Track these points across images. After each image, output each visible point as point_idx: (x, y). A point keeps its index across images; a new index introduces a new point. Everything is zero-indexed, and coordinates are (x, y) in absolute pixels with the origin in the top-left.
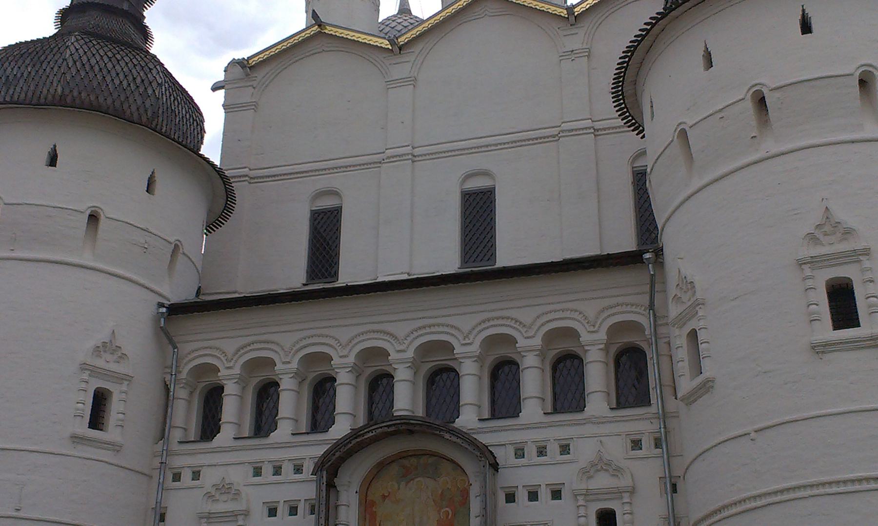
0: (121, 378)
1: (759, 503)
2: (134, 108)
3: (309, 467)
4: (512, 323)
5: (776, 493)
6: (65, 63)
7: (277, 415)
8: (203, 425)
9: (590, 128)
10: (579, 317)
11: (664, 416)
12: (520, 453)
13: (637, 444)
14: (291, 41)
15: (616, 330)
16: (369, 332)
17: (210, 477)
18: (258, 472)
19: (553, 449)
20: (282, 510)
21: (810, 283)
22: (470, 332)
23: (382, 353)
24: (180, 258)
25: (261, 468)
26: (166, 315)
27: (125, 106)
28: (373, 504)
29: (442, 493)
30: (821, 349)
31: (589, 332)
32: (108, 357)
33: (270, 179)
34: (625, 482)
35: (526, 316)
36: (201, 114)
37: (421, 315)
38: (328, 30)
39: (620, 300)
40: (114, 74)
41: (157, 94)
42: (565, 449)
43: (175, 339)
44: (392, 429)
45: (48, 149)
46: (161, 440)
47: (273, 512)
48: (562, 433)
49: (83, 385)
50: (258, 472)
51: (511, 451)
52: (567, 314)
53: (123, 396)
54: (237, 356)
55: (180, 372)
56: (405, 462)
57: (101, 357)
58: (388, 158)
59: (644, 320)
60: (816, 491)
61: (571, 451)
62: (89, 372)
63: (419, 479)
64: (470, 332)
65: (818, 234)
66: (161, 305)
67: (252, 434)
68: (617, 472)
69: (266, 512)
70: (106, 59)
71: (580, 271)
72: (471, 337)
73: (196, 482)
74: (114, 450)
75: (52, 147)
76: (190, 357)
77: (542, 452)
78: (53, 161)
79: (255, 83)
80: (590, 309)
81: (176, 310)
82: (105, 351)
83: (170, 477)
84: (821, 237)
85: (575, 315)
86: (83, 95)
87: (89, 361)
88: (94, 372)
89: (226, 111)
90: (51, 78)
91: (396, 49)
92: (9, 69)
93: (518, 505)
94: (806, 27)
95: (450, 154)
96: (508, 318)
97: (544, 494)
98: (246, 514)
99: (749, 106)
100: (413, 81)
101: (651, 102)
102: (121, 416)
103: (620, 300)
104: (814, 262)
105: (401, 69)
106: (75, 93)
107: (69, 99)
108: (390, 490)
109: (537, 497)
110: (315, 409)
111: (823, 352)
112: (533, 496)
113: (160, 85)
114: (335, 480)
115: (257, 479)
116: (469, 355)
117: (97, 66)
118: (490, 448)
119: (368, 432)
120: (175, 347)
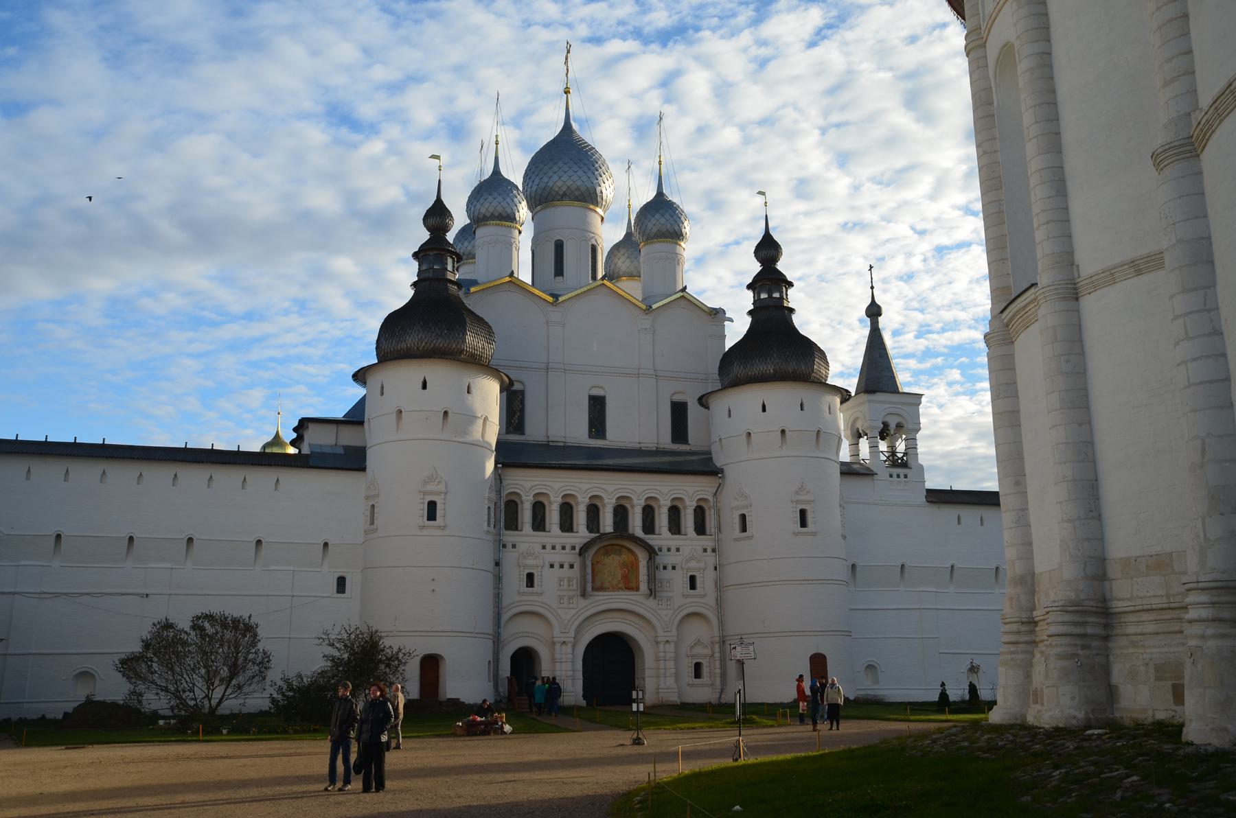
13: (705, 550)
17: (522, 547)
18: (544, 547)
20: (557, 566)
34: (702, 565)
37: (616, 482)
39: (703, 488)
42: (678, 550)
43: (502, 477)
47: (552, 566)
56: (607, 548)
59: (711, 498)
63: (613, 556)
98: (542, 567)
103: (703, 488)
112: (665, 568)
120: (501, 483)
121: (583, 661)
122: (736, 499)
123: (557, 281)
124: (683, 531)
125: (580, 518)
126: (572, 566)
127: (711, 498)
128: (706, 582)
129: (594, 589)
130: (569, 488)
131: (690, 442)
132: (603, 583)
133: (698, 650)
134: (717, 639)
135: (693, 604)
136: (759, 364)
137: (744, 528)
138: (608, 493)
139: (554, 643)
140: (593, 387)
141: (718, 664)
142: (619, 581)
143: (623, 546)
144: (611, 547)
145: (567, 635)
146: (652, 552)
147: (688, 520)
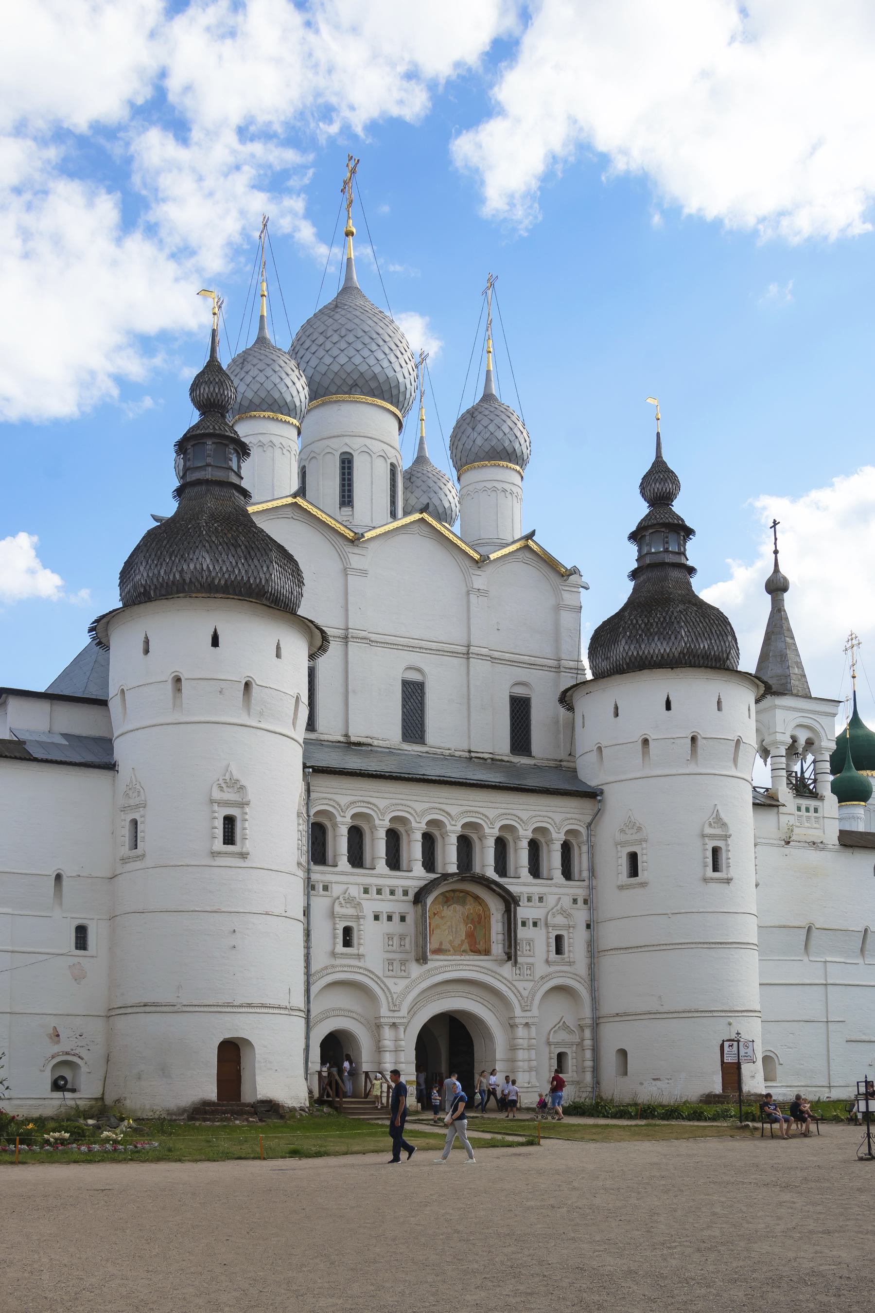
4: (517, 819)
11: (591, 888)
13: (575, 901)
17: (336, 890)
42: (541, 899)
43: (311, 788)
50: (366, 891)
56: (447, 894)
85: (550, 820)
116: (492, 835)
121: (416, 1049)
122: (622, 831)
123: (343, 513)
124: (544, 870)
125: (414, 850)
126: (403, 919)
127: (583, 831)
128: (577, 944)
130: (400, 807)
131: (534, 754)
132: (441, 943)
133: (563, 1036)
134: (589, 1021)
135: (561, 974)
136: (659, 644)
137: (634, 871)
139: (379, 1026)
140: (411, 668)
141: (588, 1054)
142: (463, 941)
143: (467, 893)
144: (452, 894)
145: (396, 1014)
146: (510, 902)
147: (553, 859)
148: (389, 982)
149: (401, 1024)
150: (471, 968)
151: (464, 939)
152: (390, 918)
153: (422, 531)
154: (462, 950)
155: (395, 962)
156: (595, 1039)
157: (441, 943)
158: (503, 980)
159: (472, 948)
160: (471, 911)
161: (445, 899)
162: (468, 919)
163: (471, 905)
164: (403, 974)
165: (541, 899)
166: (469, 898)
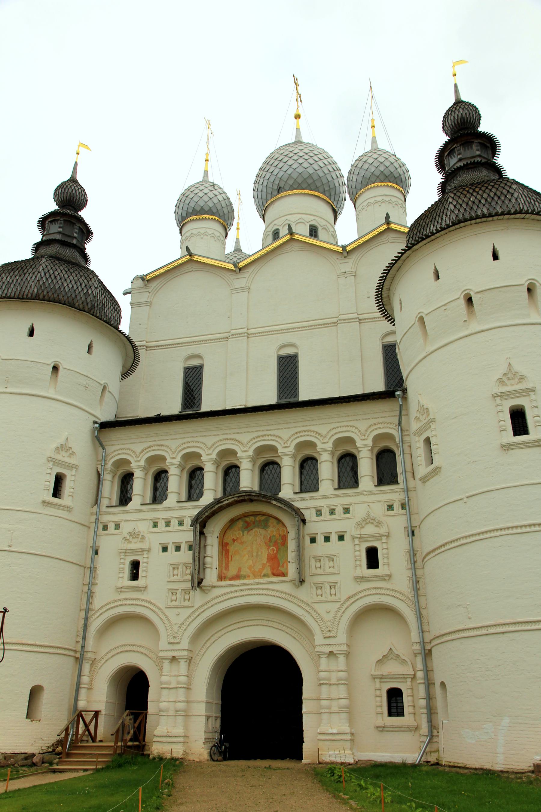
0: (71, 467)
1: (469, 540)
2: (80, 302)
3: (188, 522)
4: (314, 434)
5: (479, 534)
6: (39, 274)
7: (167, 490)
8: (121, 496)
9: (356, 318)
10: (356, 431)
11: (407, 490)
12: (319, 513)
13: (390, 507)
14: (173, 264)
15: (378, 438)
16: (225, 439)
17: (126, 528)
18: (155, 525)
19: (339, 511)
20: (171, 548)
21: (500, 408)
22: (288, 440)
23: (233, 453)
24: (107, 394)
25: (158, 523)
26: (99, 428)
27: (75, 301)
28: (227, 544)
29: (270, 537)
30: (507, 448)
31: (361, 439)
32: (63, 453)
33: (159, 348)
34: (383, 530)
35: (323, 430)
36: (119, 307)
38: (196, 258)
39: (381, 420)
40: (68, 281)
41: (94, 294)
42: (347, 511)
43: (104, 444)
44: (240, 498)
45: (29, 326)
46: (96, 505)
48: (346, 501)
49: (49, 471)
50: (155, 525)
51: (313, 512)
52: (348, 429)
53: (73, 478)
54: (142, 454)
55: (107, 464)
56: (247, 519)
57: (59, 454)
58: (233, 335)
59: (395, 433)
60: (503, 532)
61: (351, 512)
62: (53, 463)
63: (255, 529)
64: (288, 440)
65: (504, 379)
66: (95, 422)
67: (151, 502)
68: (379, 524)
69: (161, 549)
70: (64, 272)
71: (356, 402)
72: (289, 443)
73: (117, 531)
74: (68, 511)
75: (31, 325)
76: (113, 455)
77: (332, 512)
78: (31, 333)
79: (150, 290)
80: (363, 425)
81: (105, 426)
82: (62, 450)
83: (101, 527)
84: (506, 380)
86: (50, 294)
87: (53, 456)
88: (56, 462)
89: (133, 306)
90: (30, 283)
91: (238, 270)
92: (5, 278)
93: (318, 545)
94: (495, 257)
95: (270, 333)
96: (311, 431)
97: (334, 538)
98: (149, 550)
99: (462, 302)
100: (248, 289)
101: (400, 300)
102: (72, 490)
103: (381, 420)
104: (502, 395)
105: (241, 281)
106: (45, 293)
107: (41, 297)
108: (238, 536)
109: (330, 540)
110: (190, 487)
111: (508, 450)
113: (96, 288)
114: (205, 530)
115: (155, 529)
116: (289, 453)
117: (58, 276)
118: (302, 510)
119: (226, 500)
120: (104, 448)
127: (395, 433)
129: (221, 578)
132: (240, 570)
138: (241, 443)
142: (264, 566)
148: (171, 613)
149: (182, 657)
150: (261, 592)
151: (265, 562)
152: (178, 549)
153: (297, 248)
154: (262, 574)
155: (178, 592)
156: (427, 671)
157: (240, 570)
158: (300, 604)
159: (275, 572)
160: (274, 533)
161: (246, 524)
162: (270, 541)
163: (274, 526)
164: (187, 603)
165: (347, 511)
166: (272, 520)
